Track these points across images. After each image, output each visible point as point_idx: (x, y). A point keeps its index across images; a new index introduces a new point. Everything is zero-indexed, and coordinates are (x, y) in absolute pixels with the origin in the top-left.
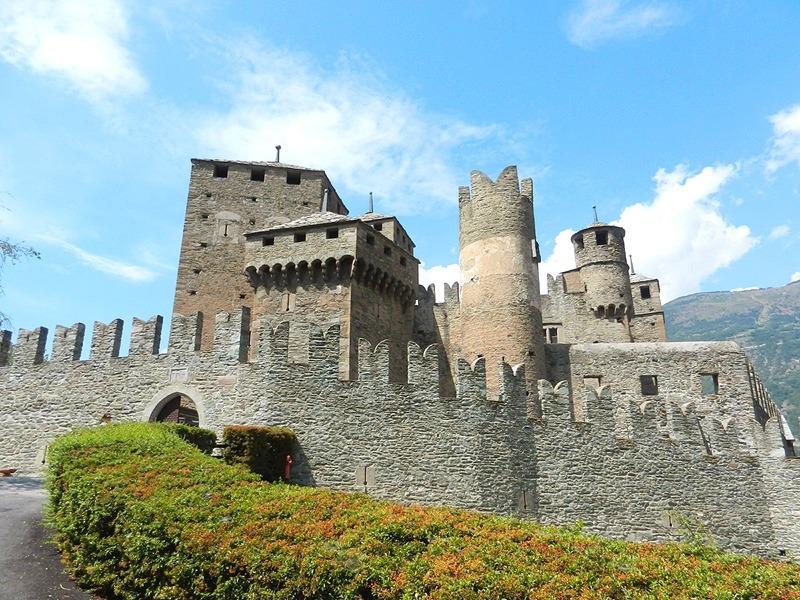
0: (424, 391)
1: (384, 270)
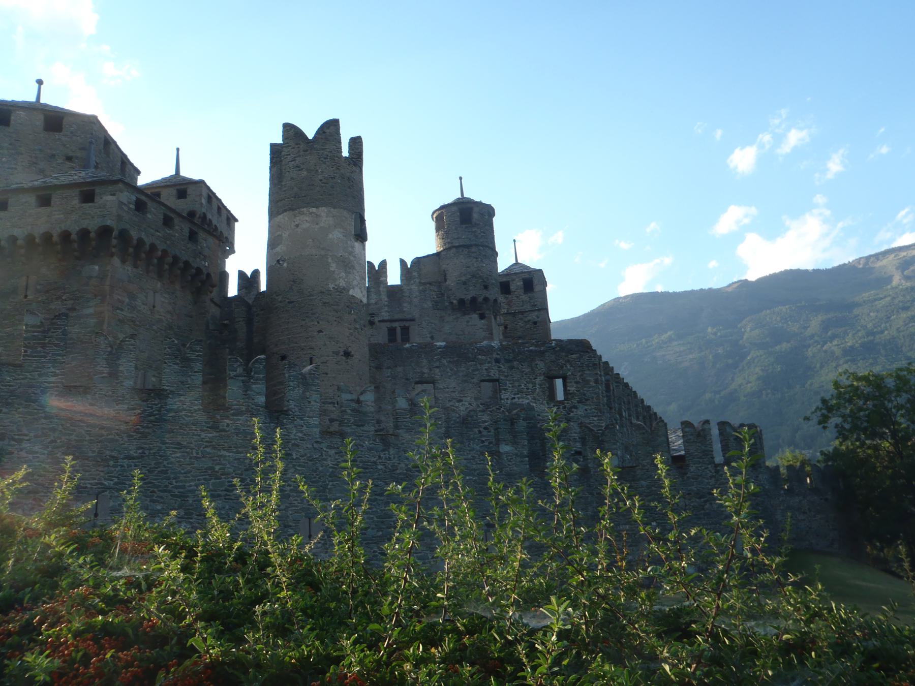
1: (161, 246)
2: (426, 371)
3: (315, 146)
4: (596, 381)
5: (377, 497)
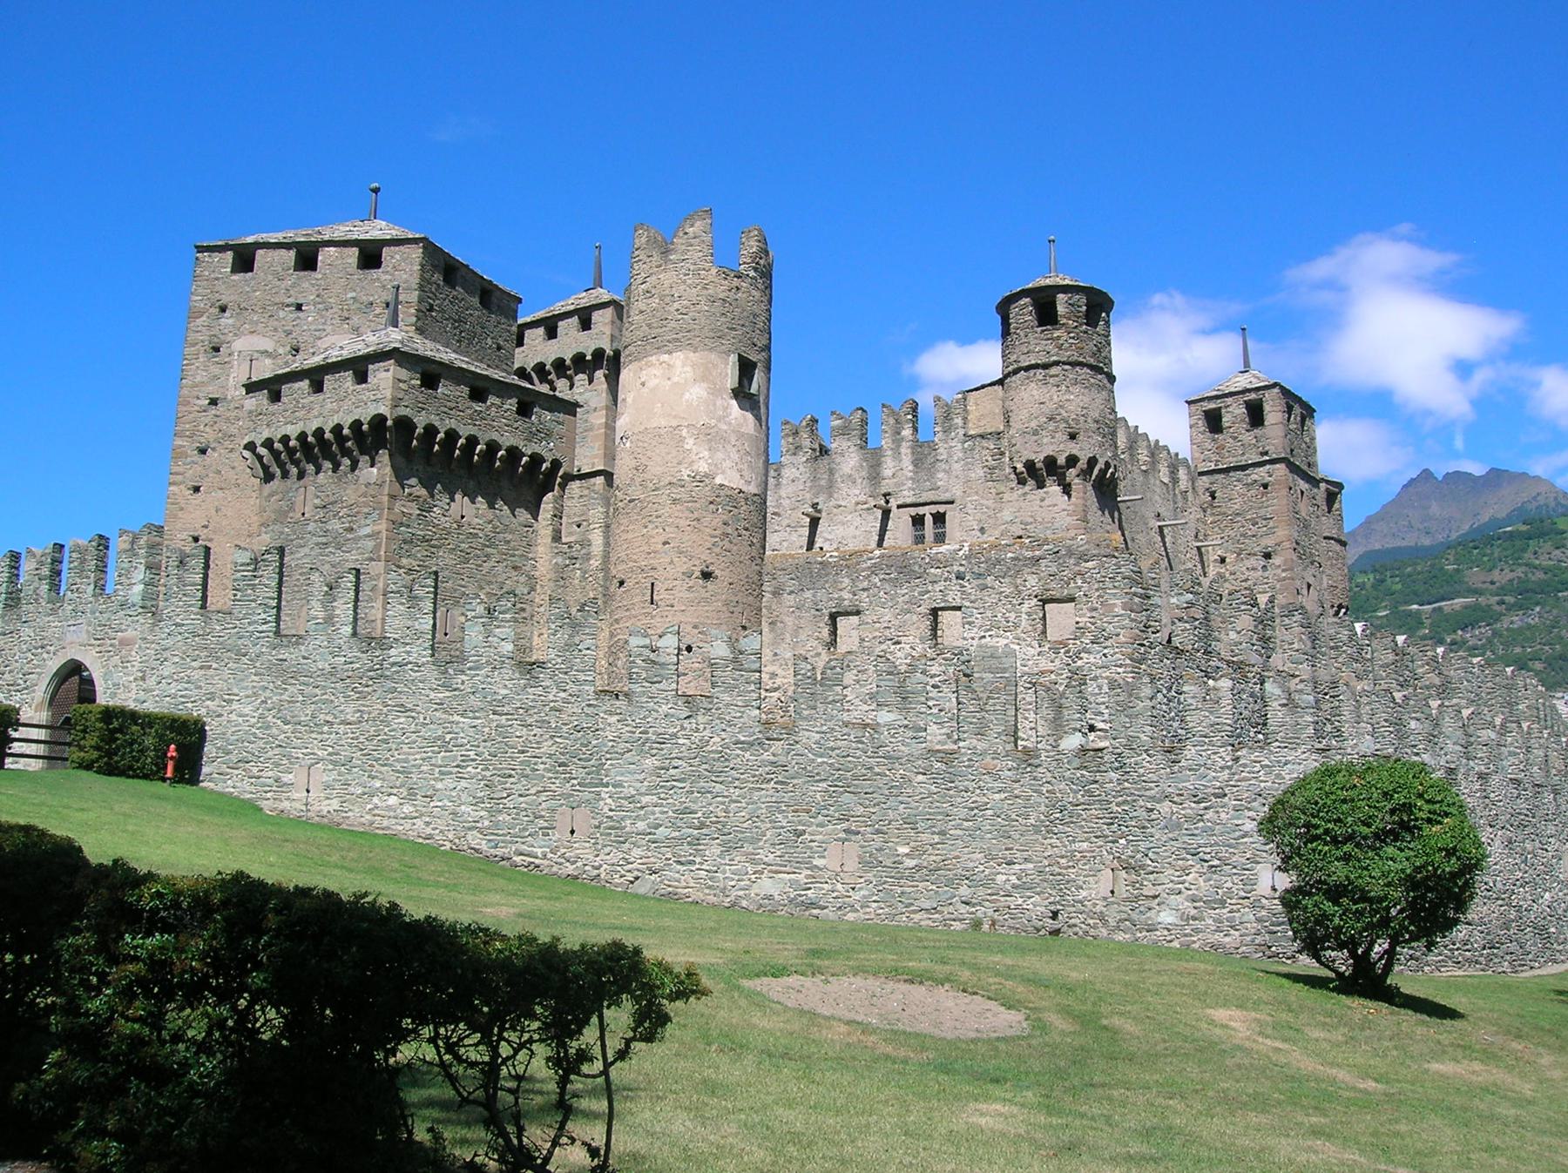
0: (408, 648)
1: (465, 431)
2: (846, 595)
3: (671, 257)
5: (674, 783)
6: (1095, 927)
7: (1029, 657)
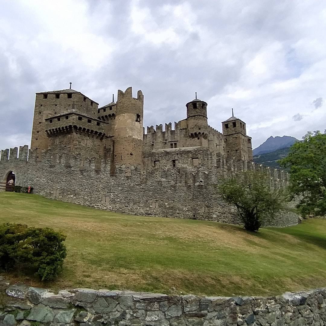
0: (75, 168)
1: (87, 128)
4: (207, 159)
6: (201, 218)
7: (190, 169)
